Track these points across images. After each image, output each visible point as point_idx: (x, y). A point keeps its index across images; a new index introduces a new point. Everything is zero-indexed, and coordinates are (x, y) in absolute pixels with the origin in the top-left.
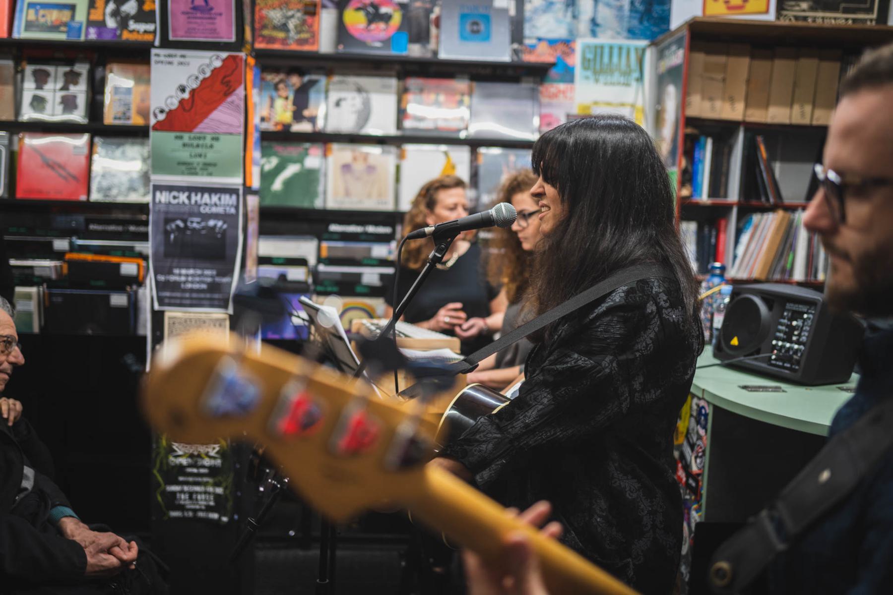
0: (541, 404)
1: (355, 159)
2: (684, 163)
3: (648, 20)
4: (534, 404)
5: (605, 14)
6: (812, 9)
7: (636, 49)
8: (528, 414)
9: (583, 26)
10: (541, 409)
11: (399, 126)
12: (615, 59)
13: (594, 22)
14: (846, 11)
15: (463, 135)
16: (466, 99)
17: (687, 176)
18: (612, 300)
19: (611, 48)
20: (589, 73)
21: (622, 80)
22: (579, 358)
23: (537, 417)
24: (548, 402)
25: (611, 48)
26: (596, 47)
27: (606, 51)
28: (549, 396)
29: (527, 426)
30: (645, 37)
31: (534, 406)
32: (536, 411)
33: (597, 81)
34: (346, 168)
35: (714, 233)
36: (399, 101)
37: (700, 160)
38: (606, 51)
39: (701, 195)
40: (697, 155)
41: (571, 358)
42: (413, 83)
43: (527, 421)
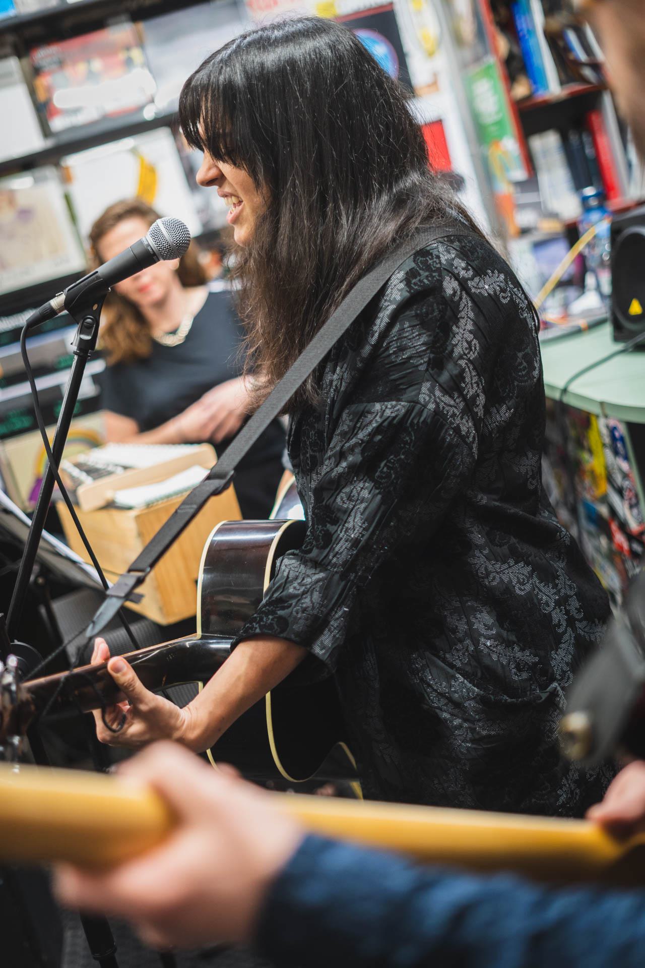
0: (362, 502)
2: (503, 45)
4: (351, 506)
8: (350, 525)
10: (365, 509)
11: (46, 132)
15: (149, 114)
16: (136, 54)
17: (515, 64)
18: (390, 301)
22: (384, 407)
23: (364, 523)
24: (369, 494)
28: (367, 485)
29: (356, 542)
31: (352, 509)
32: (359, 515)
35: (586, 139)
36: (32, 92)
37: (528, 31)
39: (546, 86)
40: (522, 24)
41: (374, 413)
42: (44, 55)
43: (352, 536)
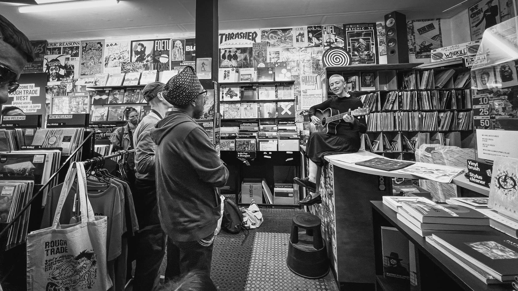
1: (247, 106)
3: (317, 69)
5: (306, 69)
6: (359, 63)
7: (315, 76)
9: (302, 72)
12: (310, 79)
13: (304, 71)
14: (368, 63)
19: (309, 76)
20: (304, 83)
21: (312, 84)
25: (309, 76)
26: (305, 77)
27: (308, 77)
30: (316, 73)
33: (306, 85)
34: (246, 108)
38: (308, 77)
